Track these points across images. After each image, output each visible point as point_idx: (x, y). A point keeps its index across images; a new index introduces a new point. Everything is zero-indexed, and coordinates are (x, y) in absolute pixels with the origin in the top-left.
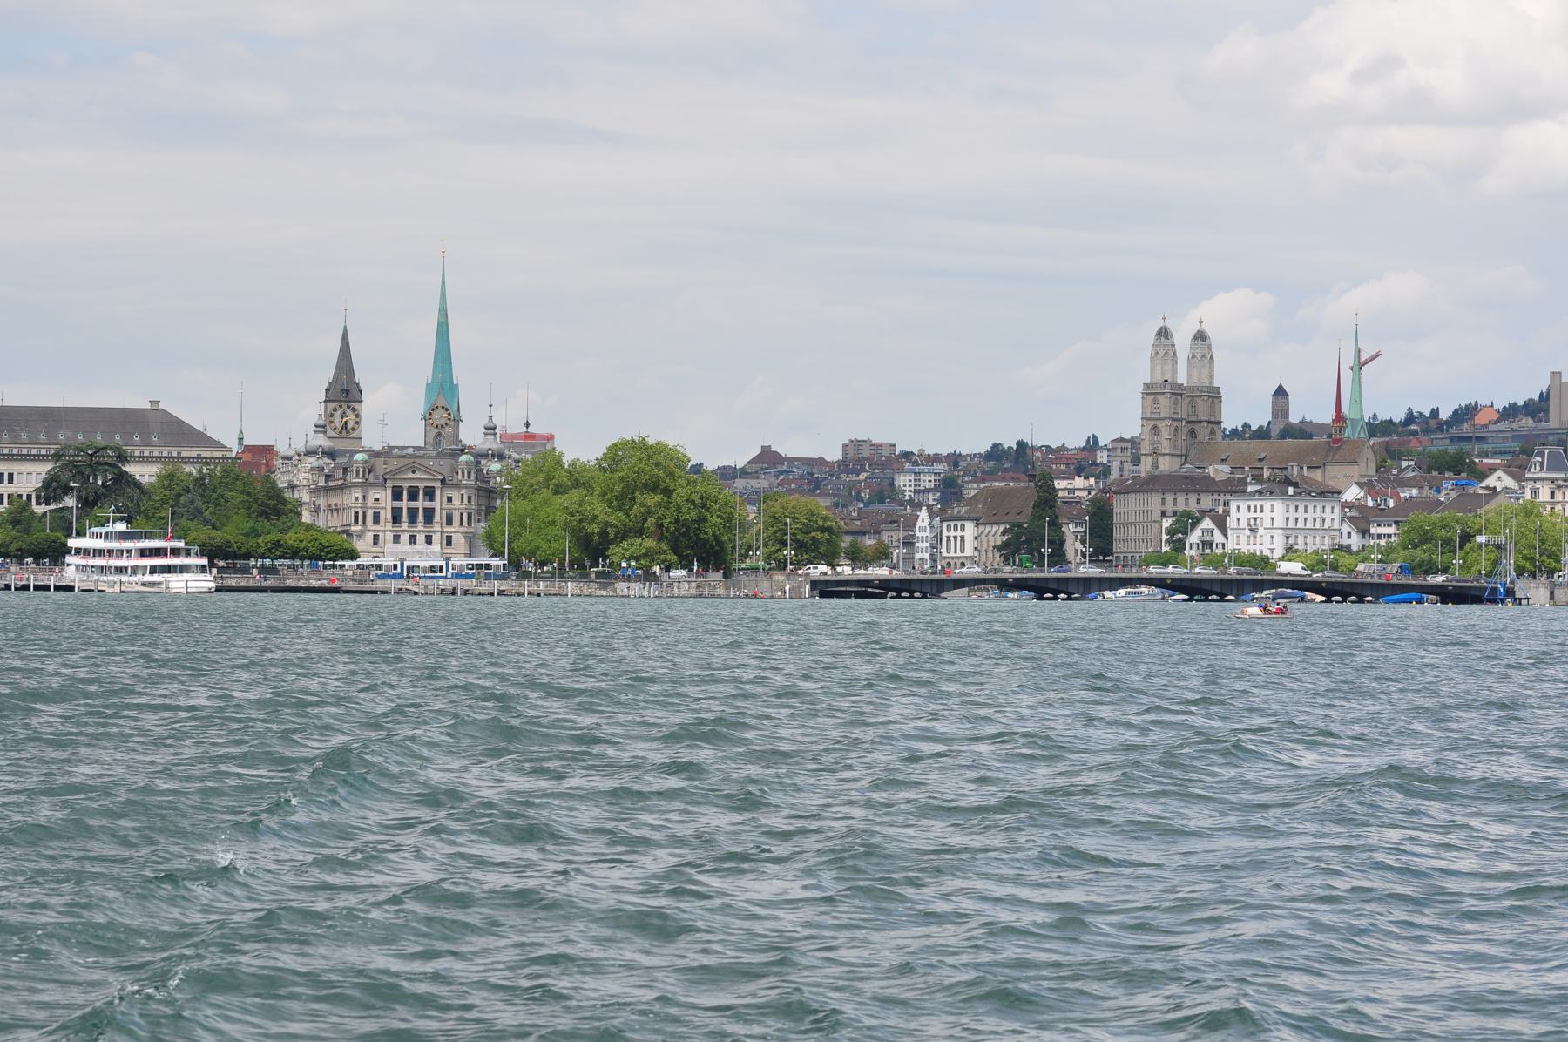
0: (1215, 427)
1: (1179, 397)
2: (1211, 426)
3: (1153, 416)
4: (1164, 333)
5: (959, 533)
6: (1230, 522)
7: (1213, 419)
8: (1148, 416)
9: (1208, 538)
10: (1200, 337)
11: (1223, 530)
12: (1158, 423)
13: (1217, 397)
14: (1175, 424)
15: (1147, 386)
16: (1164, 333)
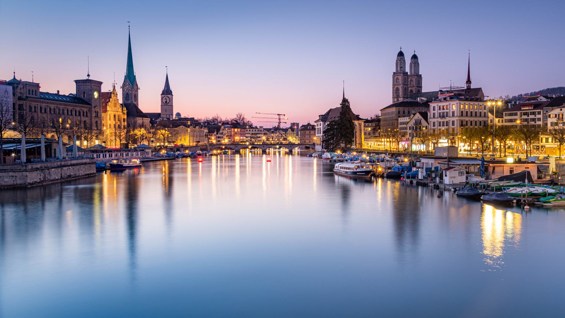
0: (420, 88)
1: (406, 77)
2: (418, 88)
4: (401, 54)
6: (430, 114)
7: (419, 86)
10: (415, 57)
11: (426, 119)
12: (398, 86)
13: (421, 78)
14: (405, 86)
15: (394, 73)
16: (401, 54)
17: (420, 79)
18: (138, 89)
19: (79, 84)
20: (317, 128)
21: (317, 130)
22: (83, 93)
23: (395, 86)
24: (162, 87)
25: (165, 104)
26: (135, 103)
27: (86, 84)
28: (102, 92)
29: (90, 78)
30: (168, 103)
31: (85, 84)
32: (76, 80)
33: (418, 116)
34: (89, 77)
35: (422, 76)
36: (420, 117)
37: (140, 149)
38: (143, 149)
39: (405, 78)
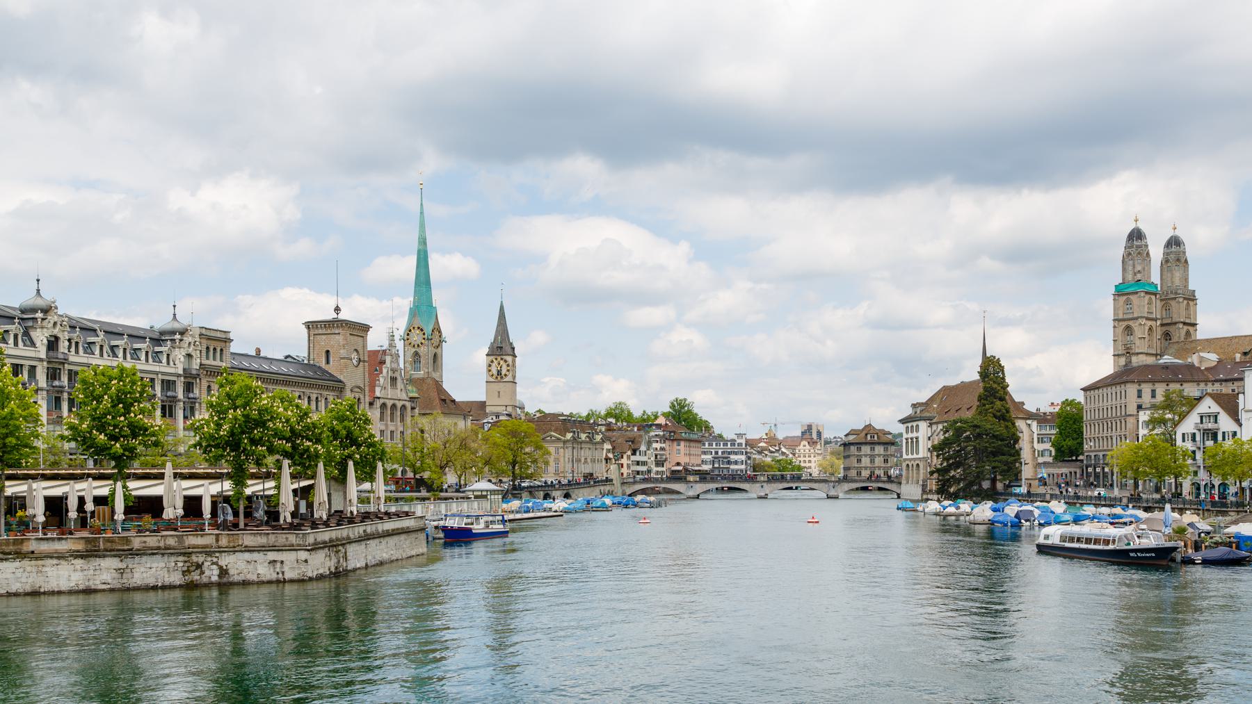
0: (1191, 329)
1: (1153, 297)
2: (1186, 328)
3: (1126, 317)
4: (1136, 236)
5: (915, 435)
7: (1188, 321)
8: (1121, 317)
9: (1210, 426)
10: (1174, 242)
11: (1234, 413)
12: (1131, 323)
13: (1193, 300)
14: (1149, 323)
17: (1191, 303)
18: (441, 342)
19: (316, 332)
20: (907, 439)
21: (907, 443)
22: (324, 354)
23: (1121, 323)
24: (490, 336)
25: (497, 378)
26: (435, 375)
27: (333, 331)
28: (369, 349)
29: (342, 316)
30: (506, 375)
31: (329, 332)
32: (308, 322)
33: (1208, 406)
34: (338, 314)
35: (1196, 294)
36: (1215, 408)
37: (476, 493)
38: (484, 493)
39: (1150, 299)
